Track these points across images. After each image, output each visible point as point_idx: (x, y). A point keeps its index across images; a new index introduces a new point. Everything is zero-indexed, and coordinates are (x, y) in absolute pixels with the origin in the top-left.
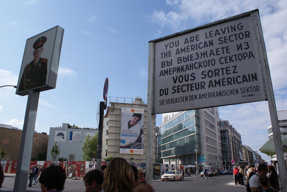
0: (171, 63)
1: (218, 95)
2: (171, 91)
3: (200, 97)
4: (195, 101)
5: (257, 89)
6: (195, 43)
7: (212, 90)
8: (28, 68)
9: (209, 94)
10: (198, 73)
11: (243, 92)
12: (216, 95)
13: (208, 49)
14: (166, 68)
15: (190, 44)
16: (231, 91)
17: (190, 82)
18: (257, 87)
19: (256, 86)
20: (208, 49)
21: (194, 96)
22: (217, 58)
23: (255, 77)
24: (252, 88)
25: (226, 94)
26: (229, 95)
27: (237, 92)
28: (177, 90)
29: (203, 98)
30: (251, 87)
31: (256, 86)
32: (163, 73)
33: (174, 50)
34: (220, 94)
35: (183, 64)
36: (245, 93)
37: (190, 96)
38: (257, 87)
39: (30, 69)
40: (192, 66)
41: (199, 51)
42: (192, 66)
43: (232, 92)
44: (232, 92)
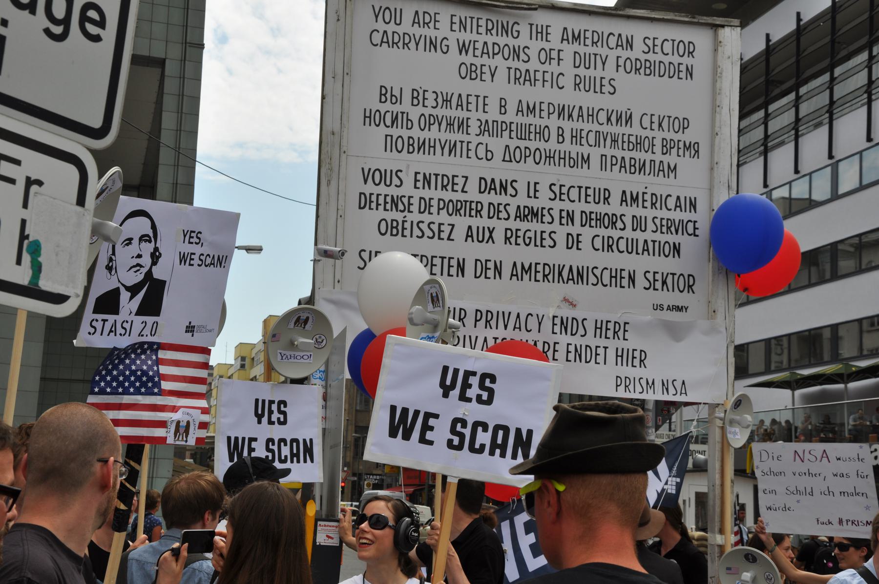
1: (573, 279)
3: (515, 273)
4: (494, 284)
5: (690, 287)
9: (547, 267)
11: (651, 286)
12: (568, 279)
16: (614, 274)
18: (691, 278)
19: (689, 275)
21: (491, 265)
24: (676, 277)
25: (599, 280)
26: (606, 286)
27: (632, 279)
29: (526, 277)
30: (673, 274)
31: (689, 275)
34: (579, 276)
36: (655, 289)
37: (476, 260)
38: (691, 278)
43: (616, 277)
44: (616, 276)
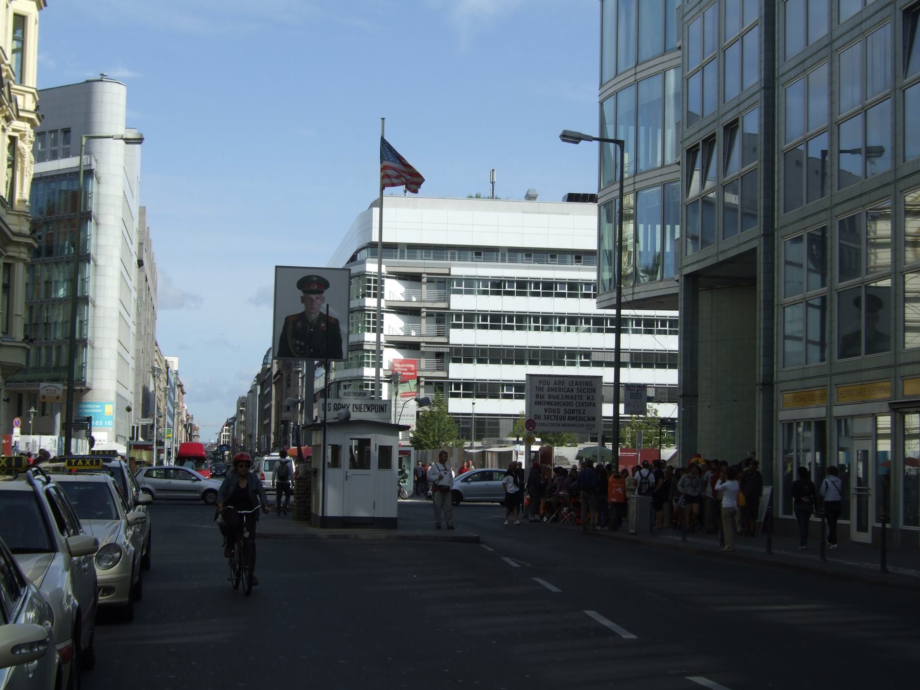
0: (543, 397)
2: (542, 417)
6: (561, 386)
7: (569, 422)
13: (570, 394)
14: (539, 400)
20: (570, 394)
22: (575, 402)
23: (594, 419)
28: (547, 418)
32: (537, 403)
34: (574, 425)
35: (552, 400)
39: (299, 324)
40: (558, 404)
41: (564, 393)
42: (558, 404)
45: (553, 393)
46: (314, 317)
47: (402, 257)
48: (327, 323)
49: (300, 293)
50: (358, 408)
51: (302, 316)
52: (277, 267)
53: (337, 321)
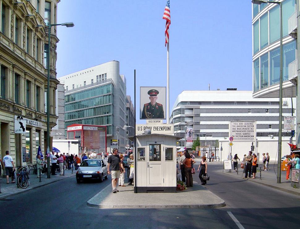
0: (235, 129)
2: (235, 136)
7: (245, 138)
8: (147, 106)
10: (242, 133)
13: (245, 128)
14: (234, 130)
15: (241, 125)
17: (240, 135)
20: (245, 128)
22: (246, 130)
33: (236, 125)
35: (238, 130)
44: (249, 139)
45: (239, 127)
46: (154, 104)
47: (189, 104)
48: (158, 106)
49: (149, 96)
50: (157, 129)
51: (150, 104)
52: (140, 87)
53: (162, 105)
